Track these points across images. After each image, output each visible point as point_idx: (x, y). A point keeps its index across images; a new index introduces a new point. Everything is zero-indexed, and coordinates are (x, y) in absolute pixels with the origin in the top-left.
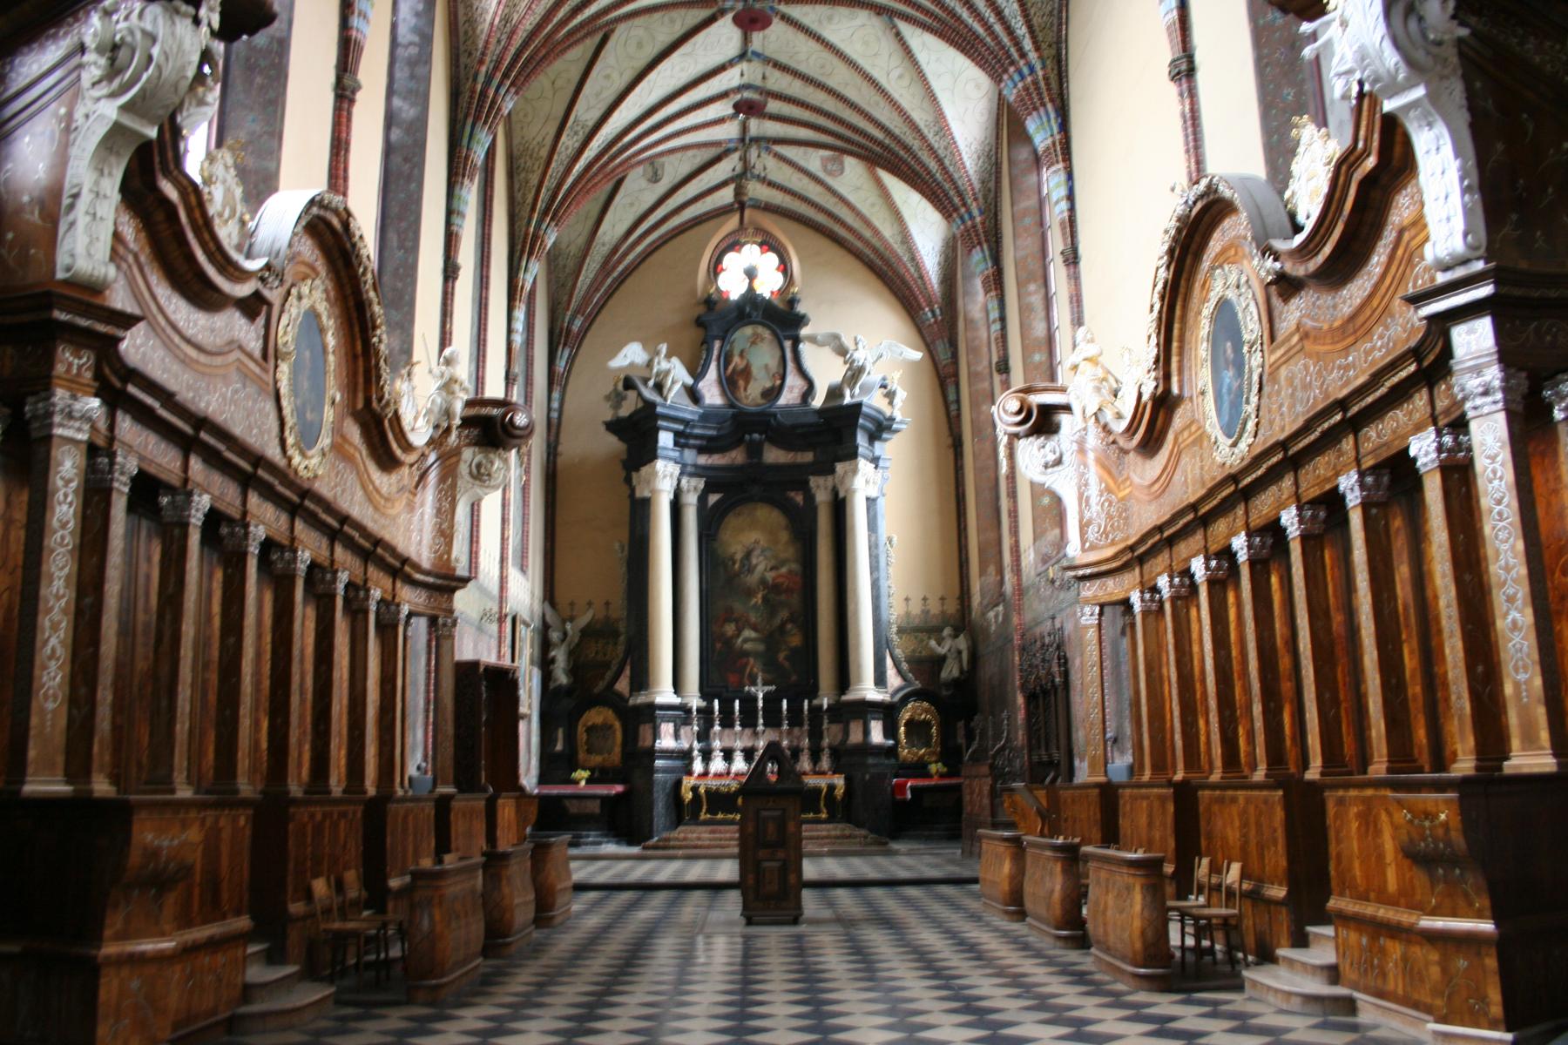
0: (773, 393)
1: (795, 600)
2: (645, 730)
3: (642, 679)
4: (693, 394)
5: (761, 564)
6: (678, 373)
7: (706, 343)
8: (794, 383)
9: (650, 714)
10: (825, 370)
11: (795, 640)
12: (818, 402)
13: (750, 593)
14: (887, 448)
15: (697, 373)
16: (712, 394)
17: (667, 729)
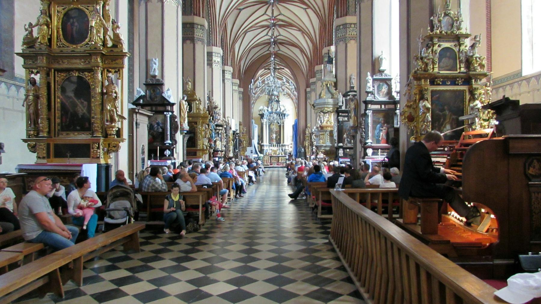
0: (276, 110)
1: (279, 133)
2: (263, 147)
3: (262, 142)
4: (268, 110)
5: (275, 129)
6: (266, 108)
7: (269, 104)
8: (279, 108)
9: (263, 145)
10: (283, 109)
11: (279, 137)
12: (281, 111)
13: (273, 132)
14: (289, 117)
15: (268, 108)
16: (270, 110)
17: (265, 147)
